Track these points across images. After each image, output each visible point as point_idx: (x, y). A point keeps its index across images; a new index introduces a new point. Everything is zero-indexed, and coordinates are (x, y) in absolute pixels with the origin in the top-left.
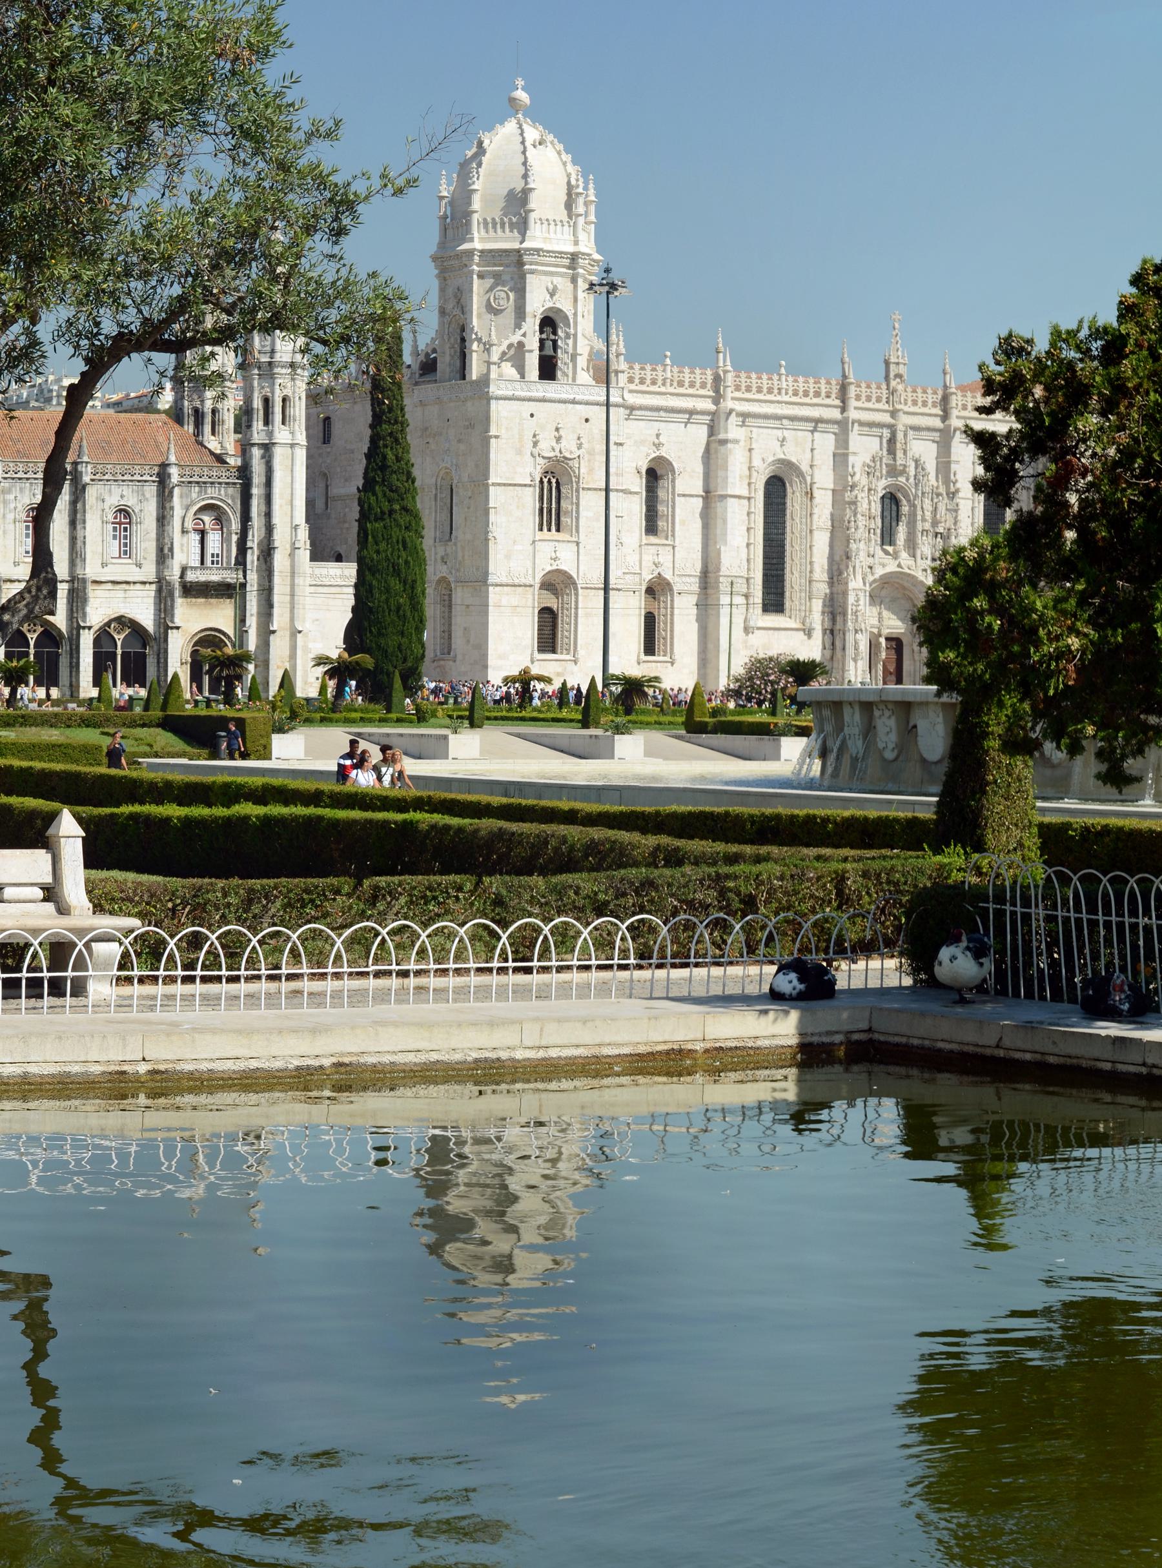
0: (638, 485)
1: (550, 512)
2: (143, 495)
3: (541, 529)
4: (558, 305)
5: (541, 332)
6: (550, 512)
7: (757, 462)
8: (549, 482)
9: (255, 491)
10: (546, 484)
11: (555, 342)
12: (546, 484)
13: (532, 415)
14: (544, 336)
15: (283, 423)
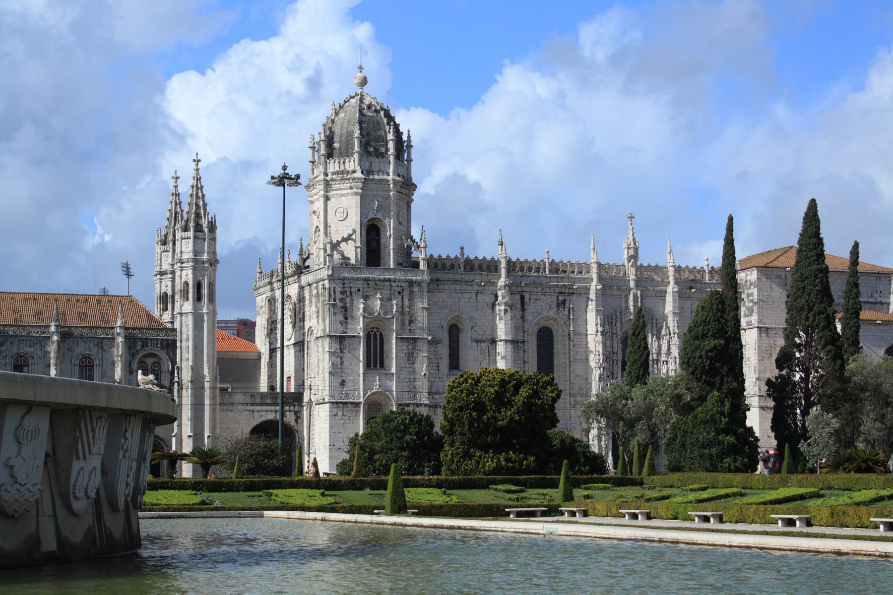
0: (445, 336)
1: (375, 352)
2: (102, 348)
3: (368, 365)
4: (378, 216)
5: (368, 234)
6: (375, 352)
7: (529, 317)
8: (375, 334)
9: (178, 344)
10: (372, 337)
11: (379, 241)
12: (372, 337)
13: (359, 290)
14: (370, 237)
15: (198, 298)
